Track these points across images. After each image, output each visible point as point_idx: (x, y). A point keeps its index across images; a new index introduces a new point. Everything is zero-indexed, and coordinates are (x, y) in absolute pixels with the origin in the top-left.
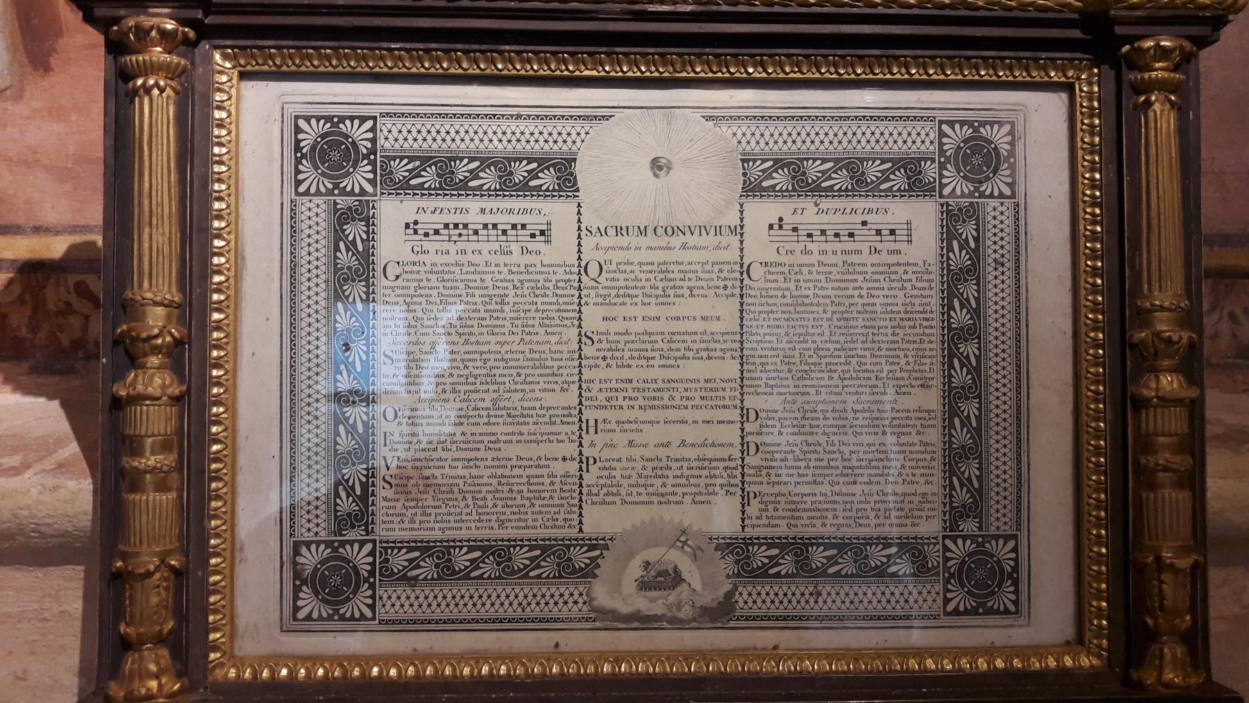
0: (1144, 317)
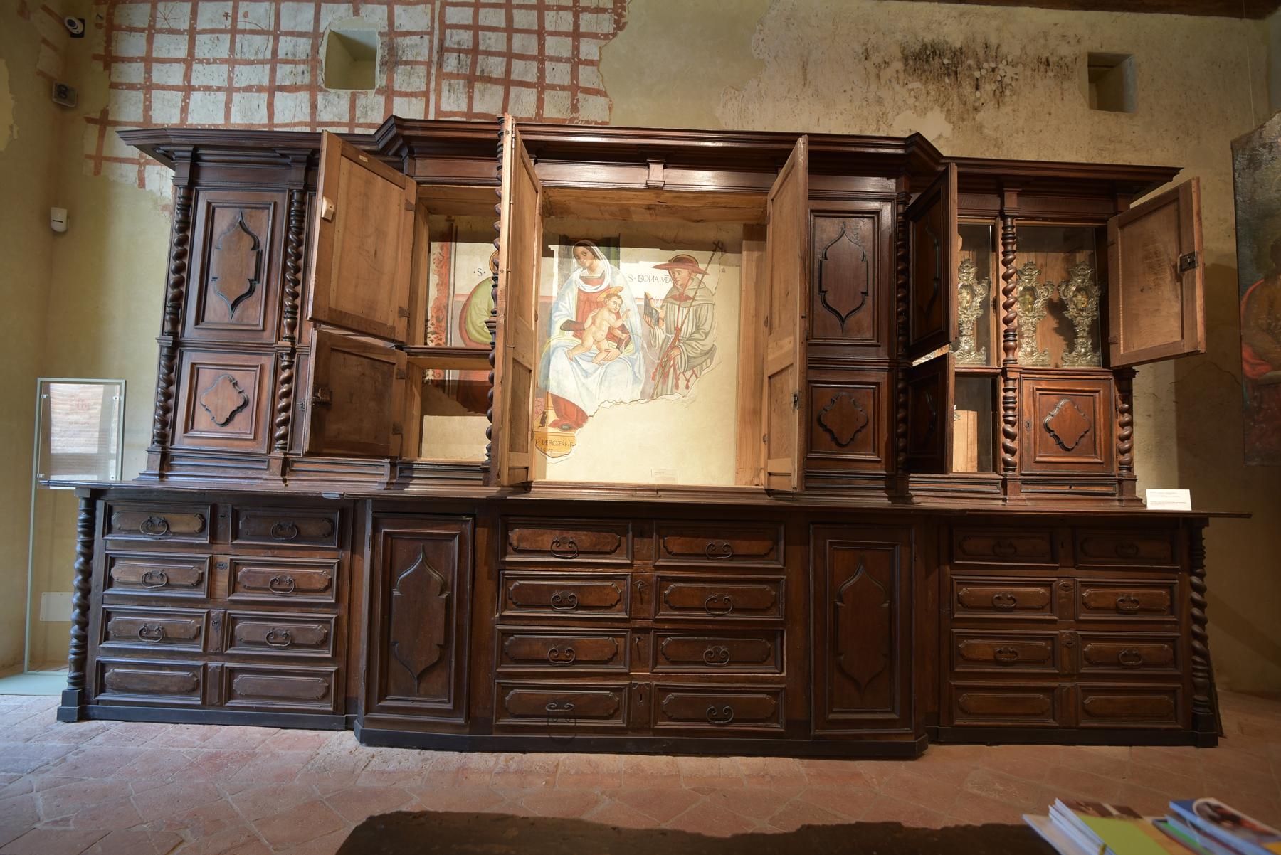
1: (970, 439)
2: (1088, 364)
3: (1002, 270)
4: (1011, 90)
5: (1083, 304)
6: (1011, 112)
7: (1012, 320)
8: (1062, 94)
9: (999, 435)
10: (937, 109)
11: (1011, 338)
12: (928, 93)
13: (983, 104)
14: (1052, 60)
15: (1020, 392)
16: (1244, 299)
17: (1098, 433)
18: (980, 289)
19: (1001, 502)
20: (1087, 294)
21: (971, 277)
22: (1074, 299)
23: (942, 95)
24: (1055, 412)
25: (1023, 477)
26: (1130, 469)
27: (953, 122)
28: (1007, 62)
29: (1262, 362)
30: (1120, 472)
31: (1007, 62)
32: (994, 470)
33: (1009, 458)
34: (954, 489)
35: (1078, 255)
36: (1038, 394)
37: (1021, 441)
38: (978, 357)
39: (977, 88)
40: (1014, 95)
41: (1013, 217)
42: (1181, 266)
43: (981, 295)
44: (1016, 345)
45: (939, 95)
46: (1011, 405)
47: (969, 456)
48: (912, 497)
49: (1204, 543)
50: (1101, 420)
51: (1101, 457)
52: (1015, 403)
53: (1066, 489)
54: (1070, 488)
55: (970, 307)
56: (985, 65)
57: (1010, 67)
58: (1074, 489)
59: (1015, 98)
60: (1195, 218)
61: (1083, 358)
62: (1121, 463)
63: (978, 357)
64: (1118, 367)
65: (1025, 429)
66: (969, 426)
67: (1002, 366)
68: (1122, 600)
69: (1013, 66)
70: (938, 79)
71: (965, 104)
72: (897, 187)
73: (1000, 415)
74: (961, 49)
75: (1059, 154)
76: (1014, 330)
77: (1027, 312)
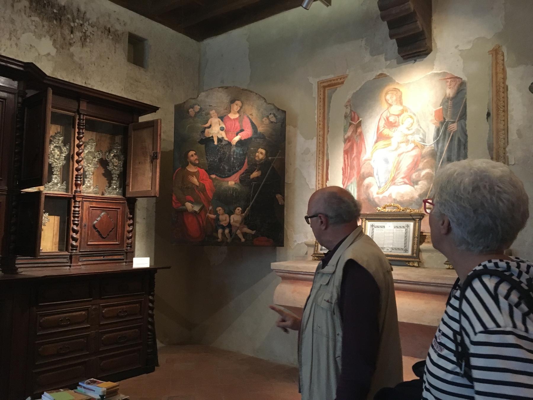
0: (415, 235)
1: (55, 232)
2: (117, 194)
3: (77, 142)
4: (90, 39)
5: (116, 163)
6: (89, 51)
7: (80, 169)
8: (115, 50)
9: (70, 231)
10: (48, 38)
11: (79, 179)
12: (43, 26)
13: (74, 42)
14: (111, 30)
15: (82, 208)
16: (175, 174)
17: (118, 229)
18: (64, 149)
19: (68, 268)
20: (118, 159)
21: (60, 142)
22: (112, 160)
23: (51, 30)
24: (99, 219)
25: (80, 253)
26: (131, 247)
27: (57, 48)
28: (89, 23)
29: (179, 202)
30: (127, 248)
31: (89, 23)
32: (67, 250)
33: (74, 243)
34: (43, 262)
35: (116, 137)
36: (91, 209)
37: (81, 234)
38: (62, 187)
39: (72, 32)
40: (91, 42)
41: (84, 115)
42: (153, 156)
43: (65, 152)
44: (81, 183)
45: (50, 30)
46: (77, 215)
47: (54, 241)
48: (17, 269)
49: (155, 280)
50: (120, 223)
51: (119, 241)
52: (79, 214)
53: (102, 258)
54: (104, 257)
55: (59, 159)
56: (77, 21)
57: (90, 26)
58: (106, 258)
59: (91, 44)
60: (159, 137)
61: (113, 193)
62: (128, 244)
63: (62, 187)
64: (129, 197)
65: (83, 228)
66: (55, 225)
67: (73, 194)
68: (120, 312)
69: (91, 26)
70: (50, 20)
71: (64, 39)
72: (18, 86)
73: (71, 220)
74: (64, 6)
75: (112, 81)
76: (81, 175)
77: (89, 165)
